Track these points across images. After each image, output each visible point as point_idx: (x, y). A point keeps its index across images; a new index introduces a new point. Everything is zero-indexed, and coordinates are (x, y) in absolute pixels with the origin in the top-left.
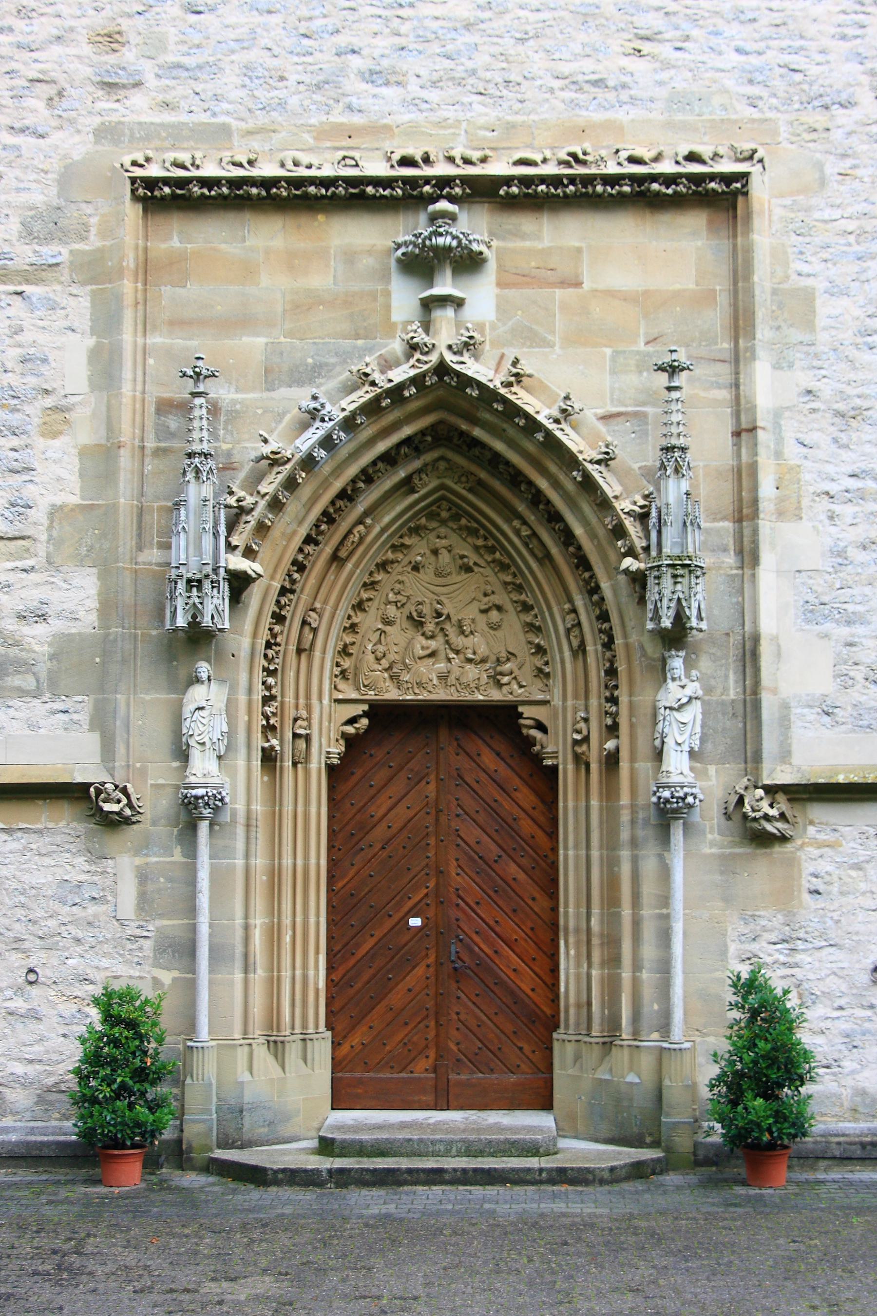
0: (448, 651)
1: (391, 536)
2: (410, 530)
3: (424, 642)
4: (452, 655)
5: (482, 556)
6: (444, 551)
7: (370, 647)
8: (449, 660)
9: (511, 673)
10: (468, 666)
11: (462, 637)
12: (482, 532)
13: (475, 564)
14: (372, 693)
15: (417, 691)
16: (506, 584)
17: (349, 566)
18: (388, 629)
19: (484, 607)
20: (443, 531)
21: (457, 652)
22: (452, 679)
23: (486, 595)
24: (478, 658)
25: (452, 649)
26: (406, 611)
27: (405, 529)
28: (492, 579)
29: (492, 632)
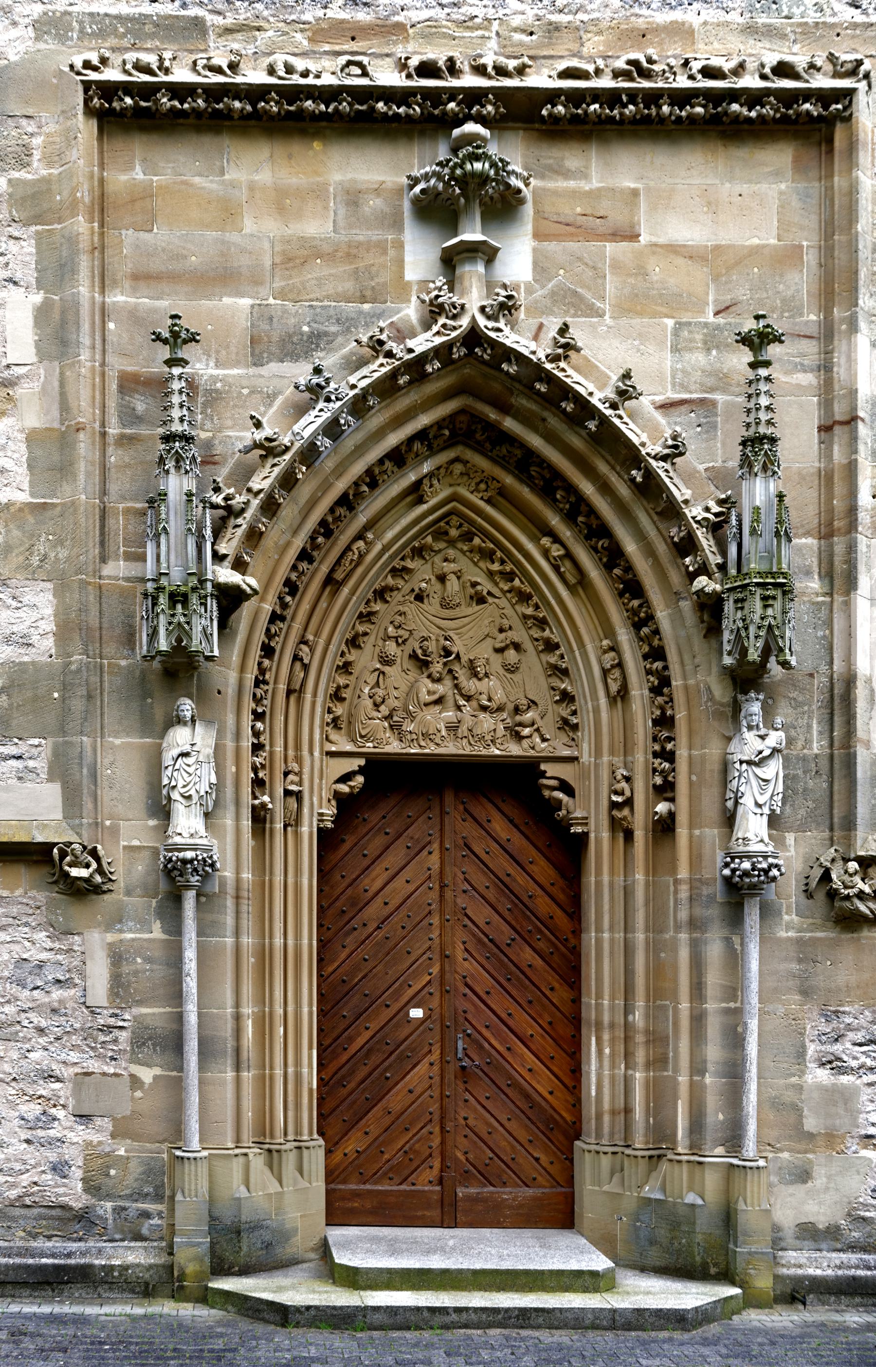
0: (458, 697)
1: (392, 558)
2: (413, 549)
3: (431, 685)
4: (462, 702)
5: (496, 584)
6: (452, 577)
7: (366, 691)
8: (459, 708)
9: (533, 724)
10: (482, 715)
11: (475, 680)
12: (499, 554)
13: (489, 593)
14: (370, 745)
15: (423, 743)
16: (525, 617)
17: (346, 591)
18: (387, 669)
19: (498, 645)
20: (451, 553)
21: (468, 698)
22: (463, 730)
23: (501, 630)
24: (493, 705)
25: (462, 695)
26: (408, 649)
27: (408, 549)
28: (509, 611)
29: (508, 676)
